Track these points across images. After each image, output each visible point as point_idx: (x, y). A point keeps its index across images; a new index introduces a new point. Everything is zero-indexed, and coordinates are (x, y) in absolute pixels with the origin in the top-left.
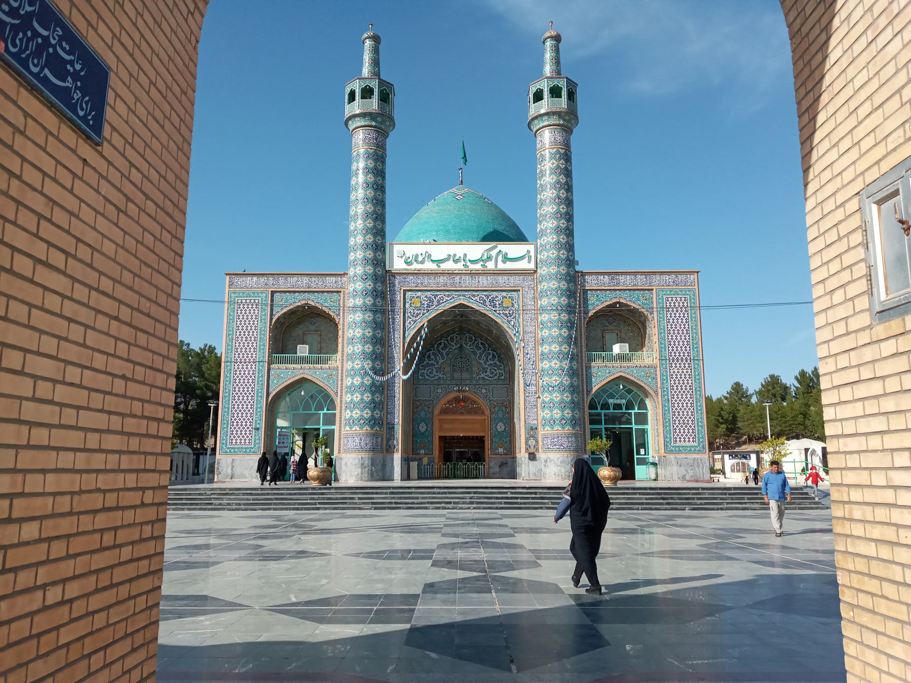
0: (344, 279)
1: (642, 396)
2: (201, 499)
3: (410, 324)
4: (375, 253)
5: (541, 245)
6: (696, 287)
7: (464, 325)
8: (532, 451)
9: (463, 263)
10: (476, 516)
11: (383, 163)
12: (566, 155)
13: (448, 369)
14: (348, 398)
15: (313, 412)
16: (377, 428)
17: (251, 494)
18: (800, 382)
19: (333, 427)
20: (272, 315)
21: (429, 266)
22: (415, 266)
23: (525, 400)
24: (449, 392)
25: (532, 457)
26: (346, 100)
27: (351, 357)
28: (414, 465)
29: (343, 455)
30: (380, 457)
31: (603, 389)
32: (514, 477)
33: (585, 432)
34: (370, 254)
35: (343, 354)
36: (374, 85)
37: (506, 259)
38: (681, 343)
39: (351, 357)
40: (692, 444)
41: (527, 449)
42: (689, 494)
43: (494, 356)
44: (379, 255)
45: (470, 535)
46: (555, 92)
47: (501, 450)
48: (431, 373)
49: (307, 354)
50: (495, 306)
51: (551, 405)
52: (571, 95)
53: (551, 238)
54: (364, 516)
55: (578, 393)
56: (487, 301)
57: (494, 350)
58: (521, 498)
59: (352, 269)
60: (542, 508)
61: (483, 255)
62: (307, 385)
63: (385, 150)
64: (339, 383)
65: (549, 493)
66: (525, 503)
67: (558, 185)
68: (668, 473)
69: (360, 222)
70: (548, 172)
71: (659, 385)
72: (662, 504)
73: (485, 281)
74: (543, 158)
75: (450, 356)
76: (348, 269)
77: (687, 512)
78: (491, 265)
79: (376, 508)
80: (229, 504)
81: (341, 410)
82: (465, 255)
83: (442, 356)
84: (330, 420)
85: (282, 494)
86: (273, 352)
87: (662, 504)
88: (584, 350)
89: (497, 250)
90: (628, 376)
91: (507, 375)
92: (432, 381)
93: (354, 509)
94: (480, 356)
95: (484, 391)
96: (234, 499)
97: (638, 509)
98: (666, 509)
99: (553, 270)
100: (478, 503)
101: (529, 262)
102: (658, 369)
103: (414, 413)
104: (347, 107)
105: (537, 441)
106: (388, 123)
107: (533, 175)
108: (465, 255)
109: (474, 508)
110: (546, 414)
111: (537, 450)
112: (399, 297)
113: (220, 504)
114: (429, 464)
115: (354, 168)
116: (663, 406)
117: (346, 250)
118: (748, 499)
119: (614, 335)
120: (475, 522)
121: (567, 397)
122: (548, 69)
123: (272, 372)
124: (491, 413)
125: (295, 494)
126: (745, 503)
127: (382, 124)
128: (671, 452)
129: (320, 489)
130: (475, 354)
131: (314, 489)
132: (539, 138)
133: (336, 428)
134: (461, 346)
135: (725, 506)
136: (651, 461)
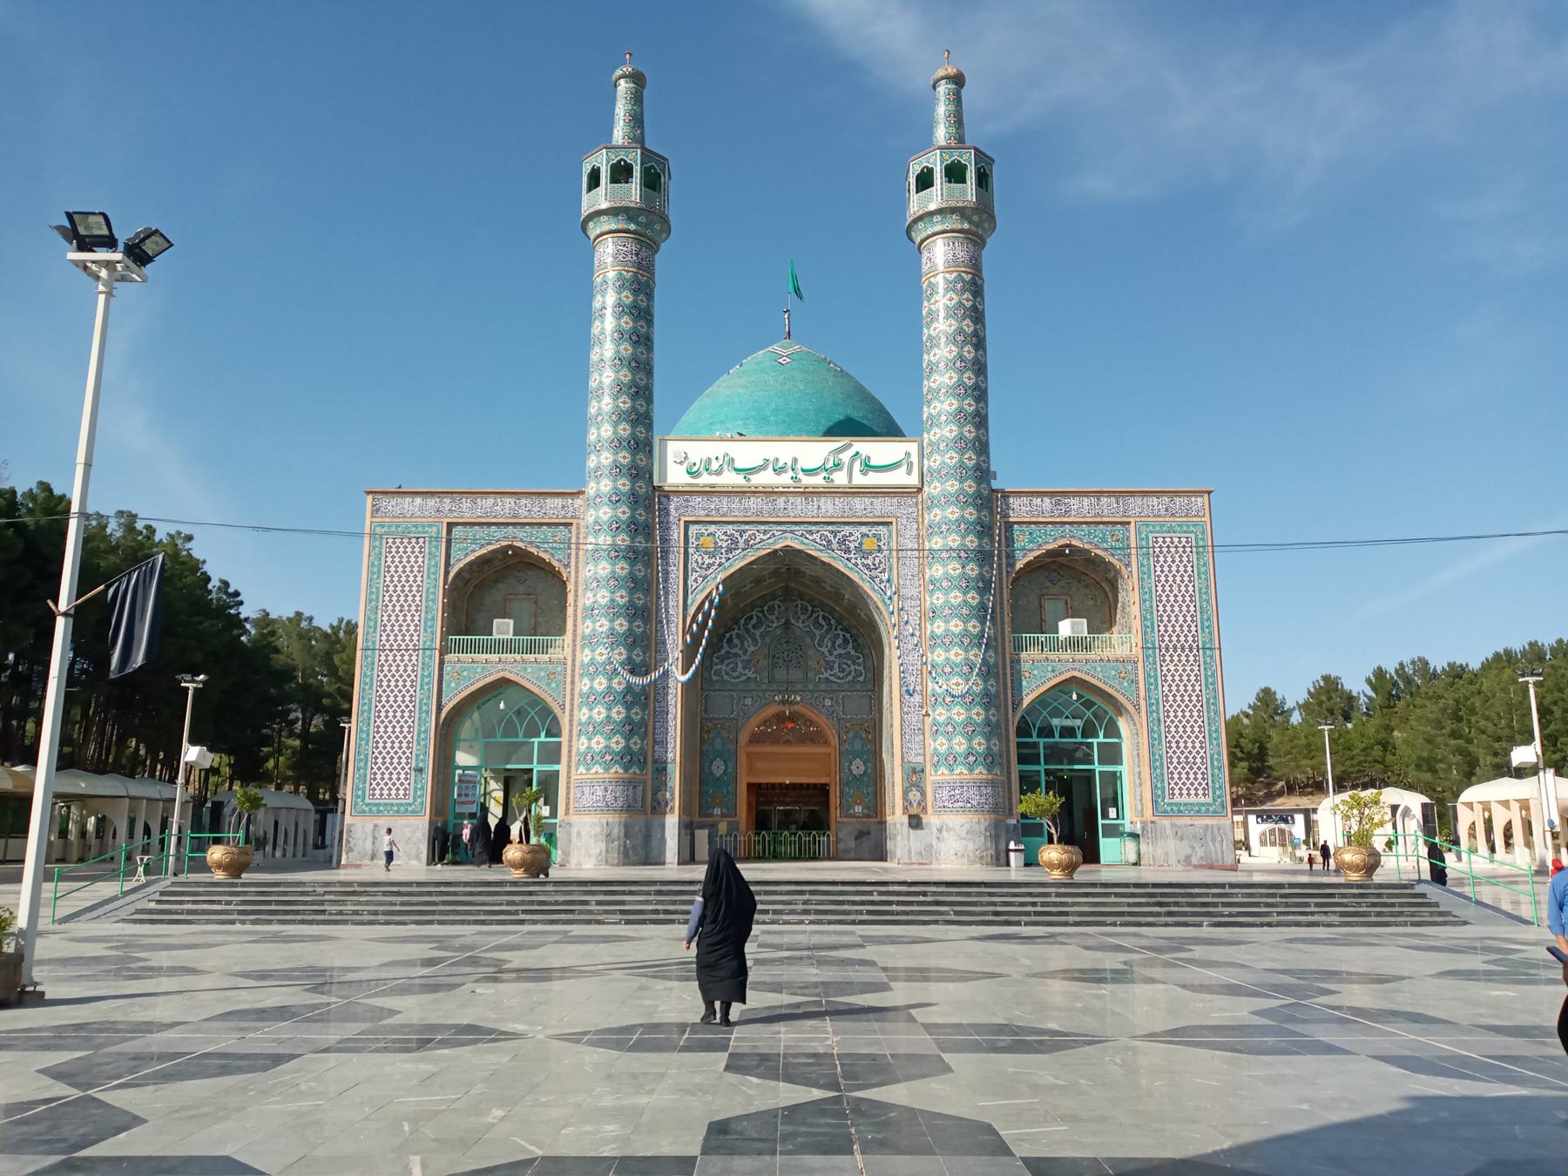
0: (579, 502)
1: (1111, 713)
2: (305, 903)
3: (696, 583)
4: (634, 455)
5: (931, 444)
6: (1207, 518)
7: (792, 585)
8: (914, 810)
9: (791, 473)
10: (816, 940)
11: (650, 296)
12: (974, 284)
13: (764, 663)
14: (583, 715)
15: (521, 739)
16: (635, 769)
17: (398, 894)
18: (1374, 688)
19: (555, 767)
20: (448, 564)
21: (730, 479)
22: (705, 479)
23: (902, 720)
24: (766, 705)
25: (915, 822)
26: (585, 186)
27: (590, 641)
28: (702, 836)
29: (574, 818)
30: (641, 819)
31: (1041, 701)
32: (883, 858)
33: (1009, 778)
34: (624, 458)
35: (575, 636)
36: (635, 158)
37: (868, 467)
38: (1181, 619)
39: (590, 641)
40: (1202, 799)
41: (905, 809)
42: (1207, 895)
43: (845, 641)
44: (642, 460)
45: (804, 987)
46: (955, 173)
47: (858, 809)
48: (734, 670)
49: (510, 636)
50: (848, 551)
51: (948, 730)
52: (983, 179)
53: (948, 431)
54: (605, 939)
55: (998, 708)
56: (835, 542)
58: (899, 903)
59: (592, 484)
60: (936, 922)
61: (826, 460)
62: (510, 691)
63: (653, 274)
64: (568, 687)
65: (950, 894)
66: (906, 913)
67: (959, 337)
68: (1160, 851)
69: (607, 400)
70: (942, 314)
71: (1142, 694)
72: (1158, 914)
73: (830, 507)
74: (933, 287)
75: (768, 640)
76: (585, 484)
77: (1206, 931)
78: (840, 478)
79: (628, 922)
80: (356, 913)
81: (571, 736)
82: (795, 460)
84: (552, 754)
85: (455, 894)
86: (449, 633)
87: (1158, 914)
88: (1007, 629)
89: (851, 452)
90: (1087, 678)
91: (870, 675)
93: (589, 922)
95: (828, 702)
96: (367, 903)
97: (1114, 924)
98: (1166, 925)
99: (952, 486)
100: (818, 912)
101: (909, 472)
102: (1140, 665)
103: (703, 741)
104: (585, 197)
105: (923, 794)
106: (657, 227)
107: (914, 321)
108: (795, 460)
109: (811, 922)
110: (940, 745)
111: (924, 809)
112: (677, 534)
113: (340, 913)
114: (729, 834)
115: (597, 304)
116: (1150, 731)
117: (581, 449)
118: (1317, 905)
119: (1060, 605)
120: (814, 954)
121: (978, 714)
122: (941, 134)
123: (447, 668)
125: (480, 894)
126: (1312, 913)
127: (647, 228)
128: (1165, 814)
129: (527, 884)
130: (813, 637)
131: (515, 883)
132: (925, 254)
133: (561, 768)
134: (787, 623)
135: (1275, 919)
136: (1128, 829)
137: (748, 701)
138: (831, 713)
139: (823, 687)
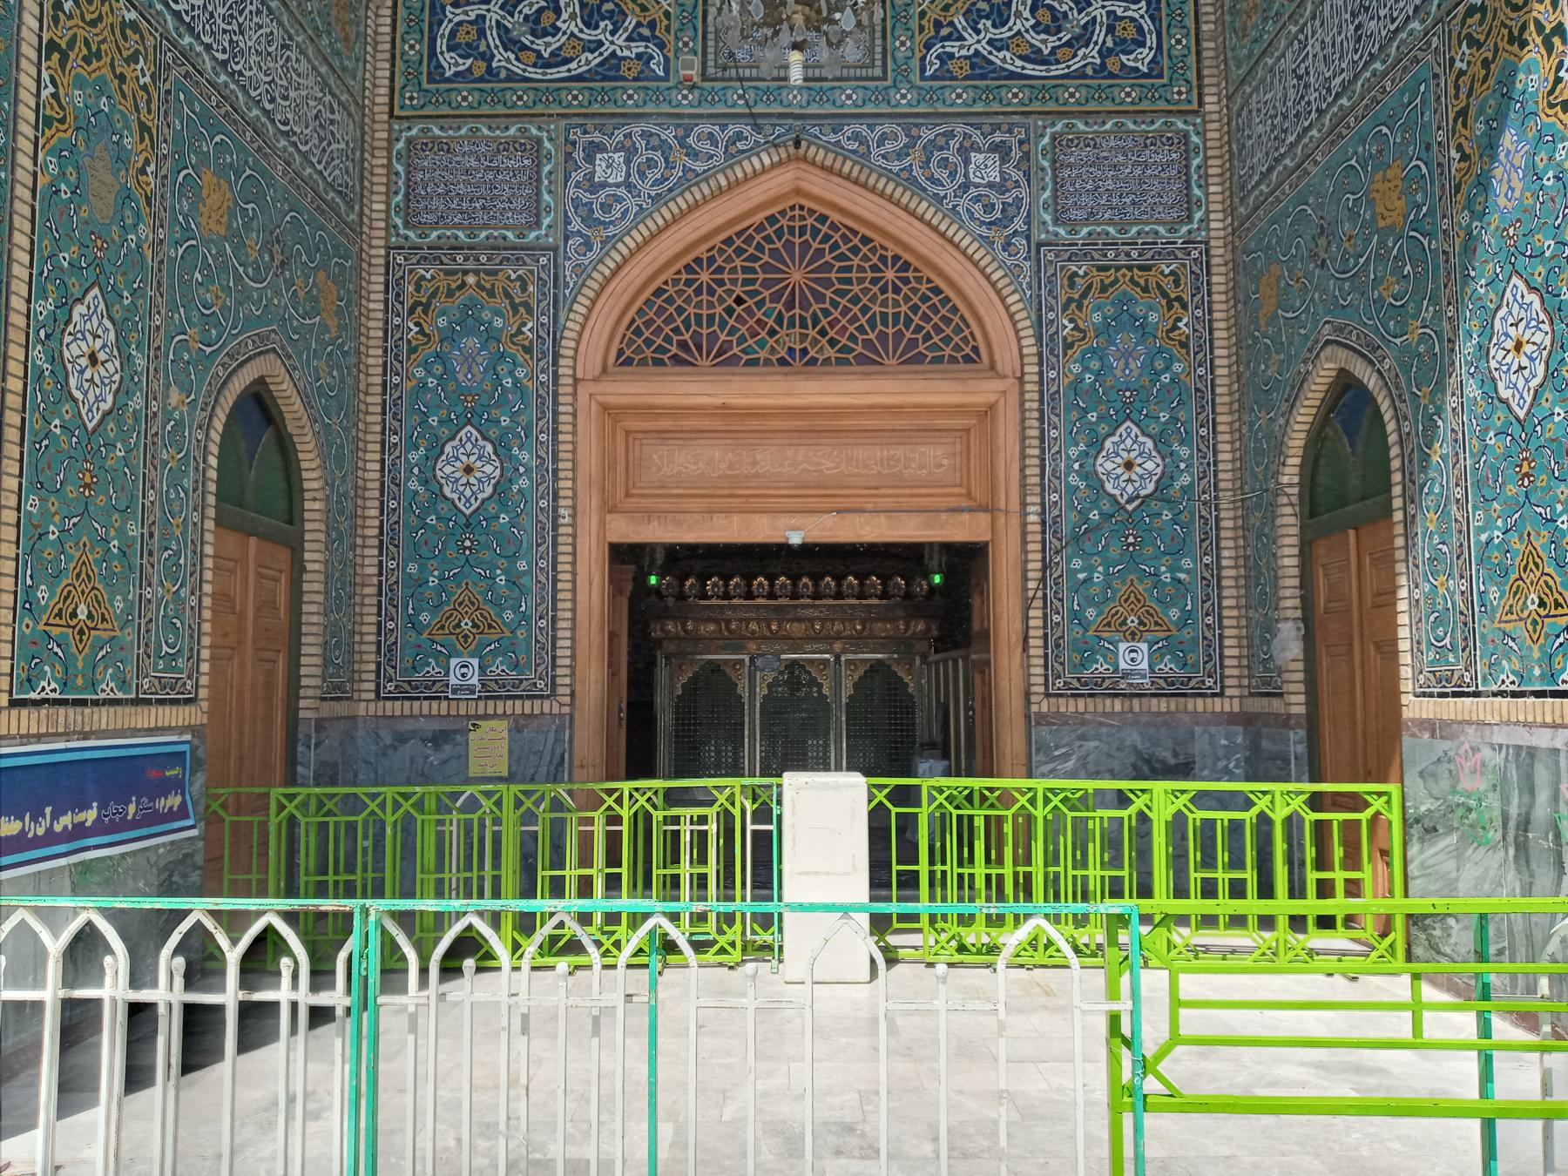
24: (690, 179)
91: (1178, 42)
92: (552, 92)
95: (984, 168)
137: (609, 169)
139: (958, 97)
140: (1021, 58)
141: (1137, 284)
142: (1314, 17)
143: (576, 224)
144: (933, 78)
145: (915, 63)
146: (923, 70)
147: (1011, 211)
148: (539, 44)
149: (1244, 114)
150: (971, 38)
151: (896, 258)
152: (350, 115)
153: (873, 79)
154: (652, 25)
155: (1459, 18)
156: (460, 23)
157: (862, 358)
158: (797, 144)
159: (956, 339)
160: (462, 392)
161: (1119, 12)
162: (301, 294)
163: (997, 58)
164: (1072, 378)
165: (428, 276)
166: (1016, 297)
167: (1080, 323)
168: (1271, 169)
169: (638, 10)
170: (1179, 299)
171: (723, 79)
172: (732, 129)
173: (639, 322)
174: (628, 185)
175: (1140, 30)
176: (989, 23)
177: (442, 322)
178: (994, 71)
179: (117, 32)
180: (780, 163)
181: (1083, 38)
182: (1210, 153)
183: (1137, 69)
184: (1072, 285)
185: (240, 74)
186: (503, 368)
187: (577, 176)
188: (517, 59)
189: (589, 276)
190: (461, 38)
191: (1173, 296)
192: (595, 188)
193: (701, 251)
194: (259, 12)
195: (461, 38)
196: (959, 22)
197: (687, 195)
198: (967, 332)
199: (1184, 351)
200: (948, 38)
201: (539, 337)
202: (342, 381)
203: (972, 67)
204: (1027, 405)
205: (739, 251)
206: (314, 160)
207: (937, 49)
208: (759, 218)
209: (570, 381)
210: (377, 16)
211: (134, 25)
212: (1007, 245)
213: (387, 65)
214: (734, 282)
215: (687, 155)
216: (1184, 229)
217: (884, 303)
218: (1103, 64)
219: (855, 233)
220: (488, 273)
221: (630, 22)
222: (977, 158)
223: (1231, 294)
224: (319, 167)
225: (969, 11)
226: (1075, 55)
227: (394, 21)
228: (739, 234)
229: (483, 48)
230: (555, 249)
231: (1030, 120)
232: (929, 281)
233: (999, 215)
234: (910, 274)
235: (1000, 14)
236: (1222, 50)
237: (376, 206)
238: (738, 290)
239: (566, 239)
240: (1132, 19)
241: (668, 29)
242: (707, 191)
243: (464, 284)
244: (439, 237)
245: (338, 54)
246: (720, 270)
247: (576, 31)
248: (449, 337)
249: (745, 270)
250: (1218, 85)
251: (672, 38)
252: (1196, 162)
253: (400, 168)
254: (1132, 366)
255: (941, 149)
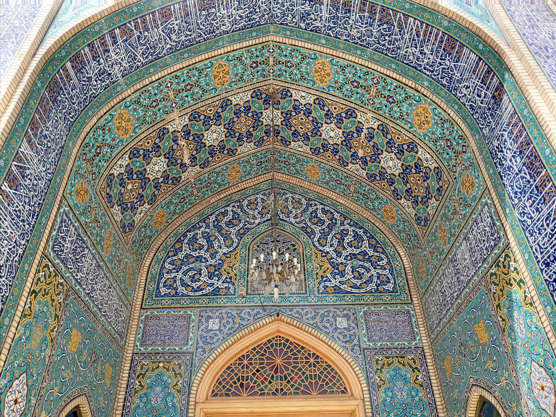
24: (241, 327)
57: (356, 224)
75: (247, 239)
83: (226, 237)
91: (401, 281)
94: (324, 235)
95: (342, 323)
124: (373, 388)
137: (214, 324)
138: (349, 339)
139: (331, 299)
140: (350, 287)
141: (401, 363)
142: (443, 275)
143: (201, 344)
144: (322, 293)
145: (316, 289)
146: (318, 291)
147: (353, 337)
148: (193, 285)
149: (427, 304)
150: (333, 281)
151: (314, 354)
152: (127, 308)
153: (303, 294)
154: (231, 278)
155: (489, 277)
156: (168, 279)
157: (304, 391)
158: (278, 315)
159: (338, 384)
160: (153, 409)
161: (380, 273)
162: (99, 372)
163: (342, 287)
164: (382, 399)
165: (146, 364)
166: (358, 368)
167: (382, 378)
168: (439, 322)
169: (226, 274)
170: (416, 368)
171: (253, 295)
172: (255, 311)
173: (221, 379)
174: (220, 330)
175: (388, 278)
176: (339, 276)
177: (148, 381)
178: (342, 291)
179: (56, 286)
180: (272, 321)
181: (370, 280)
182: (418, 317)
183: (389, 290)
184: (377, 364)
185: (93, 297)
186: (169, 399)
187: (202, 327)
188: (186, 289)
189: (204, 363)
190: (168, 283)
191: (414, 367)
192: (208, 331)
193: (244, 353)
194: (103, 277)
195: (168, 283)
196: (329, 276)
197: (240, 333)
198: (341, 382)
199: (422, 388)
200: (326, 281)
201: (184, 386)
202: (108, 405)
203: (335, 290)
204: (367, 411)
205: (258, 352)
206: (112, 324)
207: (323, 284)
208: (265, 340)
209: (194, 403)
210: (141, 276)
211: (62, 284)
212: (352, 350)
213: (142, 292)
214: (256, 363)
215: (241, 319)
216: (414, 343)
217: (310, 371)
218: (378, 289)
219: (299, 345)
220: (167, 362)
221: (224, 277)
222: (339, 319)
223: (435, 366)
224: (114, 326)
225: (332, 273)
226: (368, 286)
227: (147, 278)
228: (258, 346)
229: (175, 286)
230: (192, 353)
231: (356, 307)
232: (326, 362)
233: (349, 339)
234: (319, 360)
235: (342, 274)
236: (416, 284)
237: (131, 339)
238: (257, 367)
239: (197, 349)
240: (385, 275)
241: (236, 279)
242: (247, 332)
243: (158, 366)
244: (152, 350)
245: (127, 289)
246: (251, 359)
247: (206, 280)
248: (151, 387)
249: (260, 359)
250: (416, 295)
251: (237, 282)
252: (414, 320)
253: (141, 326)
254: (404, 394)
255: (327, 316)
